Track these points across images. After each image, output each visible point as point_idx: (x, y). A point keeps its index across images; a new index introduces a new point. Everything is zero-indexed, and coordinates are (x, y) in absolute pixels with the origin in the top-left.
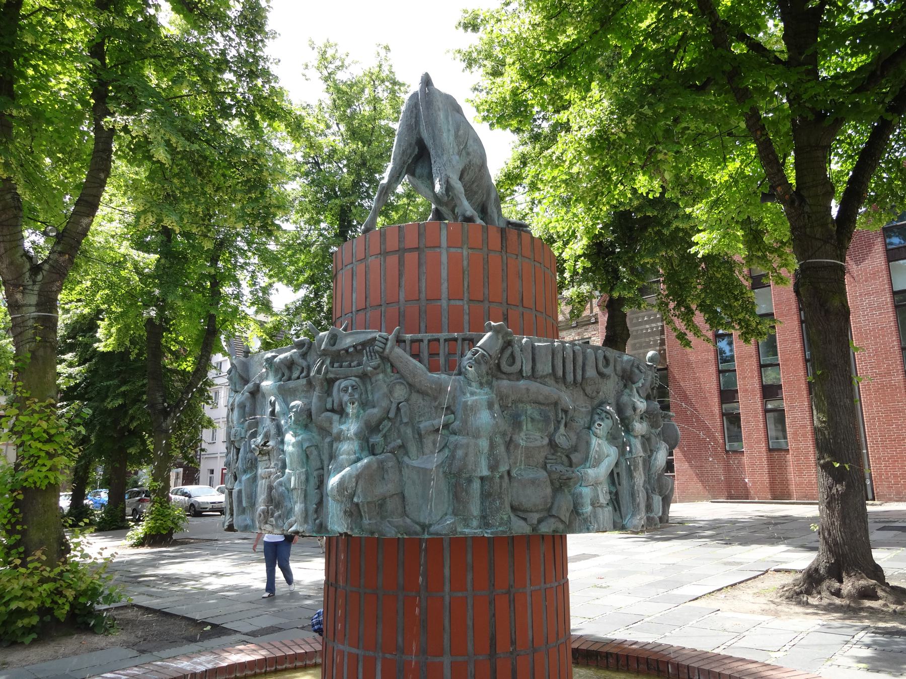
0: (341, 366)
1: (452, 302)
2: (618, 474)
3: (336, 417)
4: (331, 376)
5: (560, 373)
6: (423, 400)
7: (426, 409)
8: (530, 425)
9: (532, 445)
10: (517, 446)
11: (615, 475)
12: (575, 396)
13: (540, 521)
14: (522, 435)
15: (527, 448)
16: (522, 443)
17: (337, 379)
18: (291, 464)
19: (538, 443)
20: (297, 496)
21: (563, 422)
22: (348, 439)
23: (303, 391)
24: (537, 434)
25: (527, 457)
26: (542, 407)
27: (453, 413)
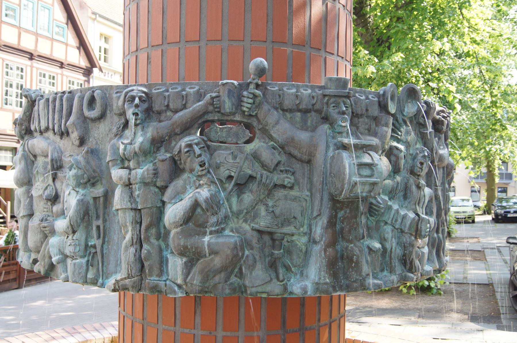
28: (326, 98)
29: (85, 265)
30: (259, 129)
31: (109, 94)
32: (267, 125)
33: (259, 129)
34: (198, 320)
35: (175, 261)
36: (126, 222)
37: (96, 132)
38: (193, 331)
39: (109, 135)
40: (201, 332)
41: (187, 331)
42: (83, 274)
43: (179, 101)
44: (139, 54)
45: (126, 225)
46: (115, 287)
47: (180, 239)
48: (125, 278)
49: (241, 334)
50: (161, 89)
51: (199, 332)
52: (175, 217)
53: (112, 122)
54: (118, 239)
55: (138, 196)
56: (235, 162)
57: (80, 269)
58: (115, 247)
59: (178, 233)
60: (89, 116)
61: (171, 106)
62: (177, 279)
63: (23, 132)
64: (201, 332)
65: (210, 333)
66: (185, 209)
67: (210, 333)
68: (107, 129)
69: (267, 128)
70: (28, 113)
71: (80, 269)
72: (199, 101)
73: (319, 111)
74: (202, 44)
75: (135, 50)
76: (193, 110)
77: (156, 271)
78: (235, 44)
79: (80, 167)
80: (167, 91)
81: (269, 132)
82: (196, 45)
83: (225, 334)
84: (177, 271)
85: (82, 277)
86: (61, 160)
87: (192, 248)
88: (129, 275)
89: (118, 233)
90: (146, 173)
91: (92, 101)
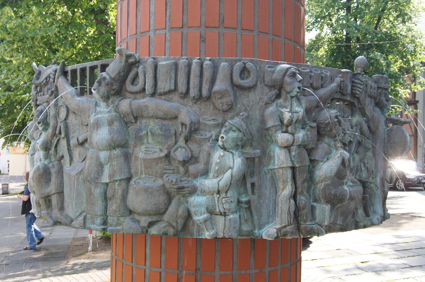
1: (157, 32)
2: (253, 185)
4: (38, 103)
5: (182, 88)
7: (77, 127)
8: (150, 140)
9: (149, 157)
10: (137, 158)
11: (249, 186)
12: (203, 109)
13: (151, 224)
14: (143, 148)
15: (145, 160)
16: (141, 155)
19: (156, 156)
21: (183, 135)
24: (156, 147)
25: (146, 168)
26: (166, 122)
28: (380, 90)
29: (238, 220)
30: (358, 108)
31: (260, 67)
32: (365, 106)
33: (358, 108)
34: (252, 261)
35: (323, 207)
36: (287, 178)
37: (245, 99)
38: (248, 272)
39: (260, 104)
40: (254, 271)
41: (243, 272)
42: (238, 228)
43: (320, 81)
44: (185, 30)
45: (287, 181)
46: (278, 235)
47: (332, 189)
48: (285, 226)
49: (279, 267)
50: (306, 69)
51: (253, 271)
52: (331, 171)
53: (262, 92)
54: (270, 193)
55: (294, 156)
56: (353, 130)
57: (235, 223)
58: (267, 201)
59: (328, 185)
60: (243, 84)
61: (315, 84)
62: (324, 221)
63: (112, 92)
64: (254, 271)
65: (261, 270)
66: (338, 166)
67: (261, 270)
68: (258, 98)
69: (365, 107)
70: (122, 73)
71: (235, 223)
72: (331, 83)
73: (375, 99)
74: (255, 33)
75: (181, 26)
76: (332, 89)
77: (310, 216)
78: (276, 38)
79: (241, 130)
80: (311, 72)
81: (365, 110)
82: (250, 33)
83: (270, 269)
84: (325, 216)
85: (237, 231)
86: (199, 122)
87: (340, 196)
88: (288, 223)
89: (270, 189)
90: (306, 137)
91: (244, 71)
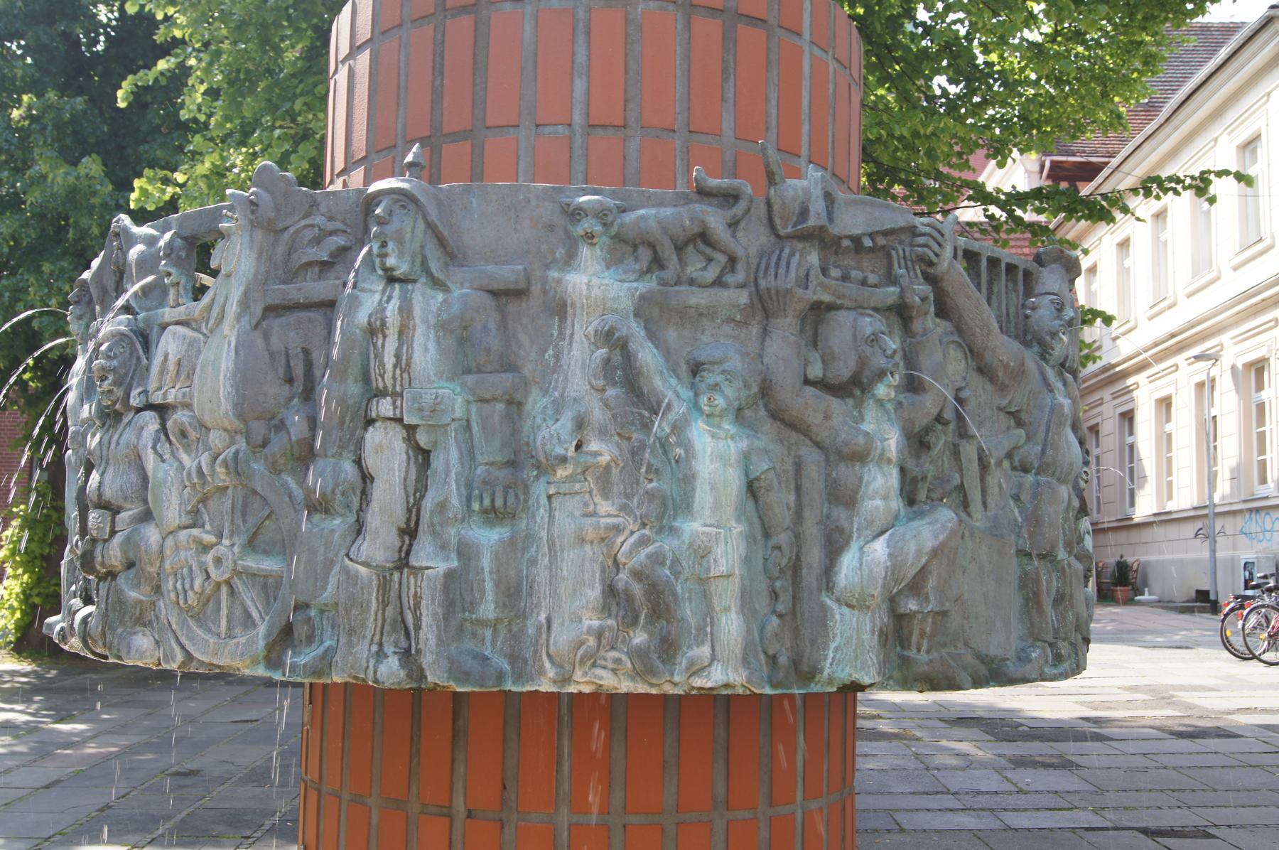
0: (845, 278)
3: (835, 404)
6: (983, 388)
17: (832, 307)
18: (716, 508)
20: (727, 597)
22: (882, 459)
23: (730, 320)
27: (1019, 424)
